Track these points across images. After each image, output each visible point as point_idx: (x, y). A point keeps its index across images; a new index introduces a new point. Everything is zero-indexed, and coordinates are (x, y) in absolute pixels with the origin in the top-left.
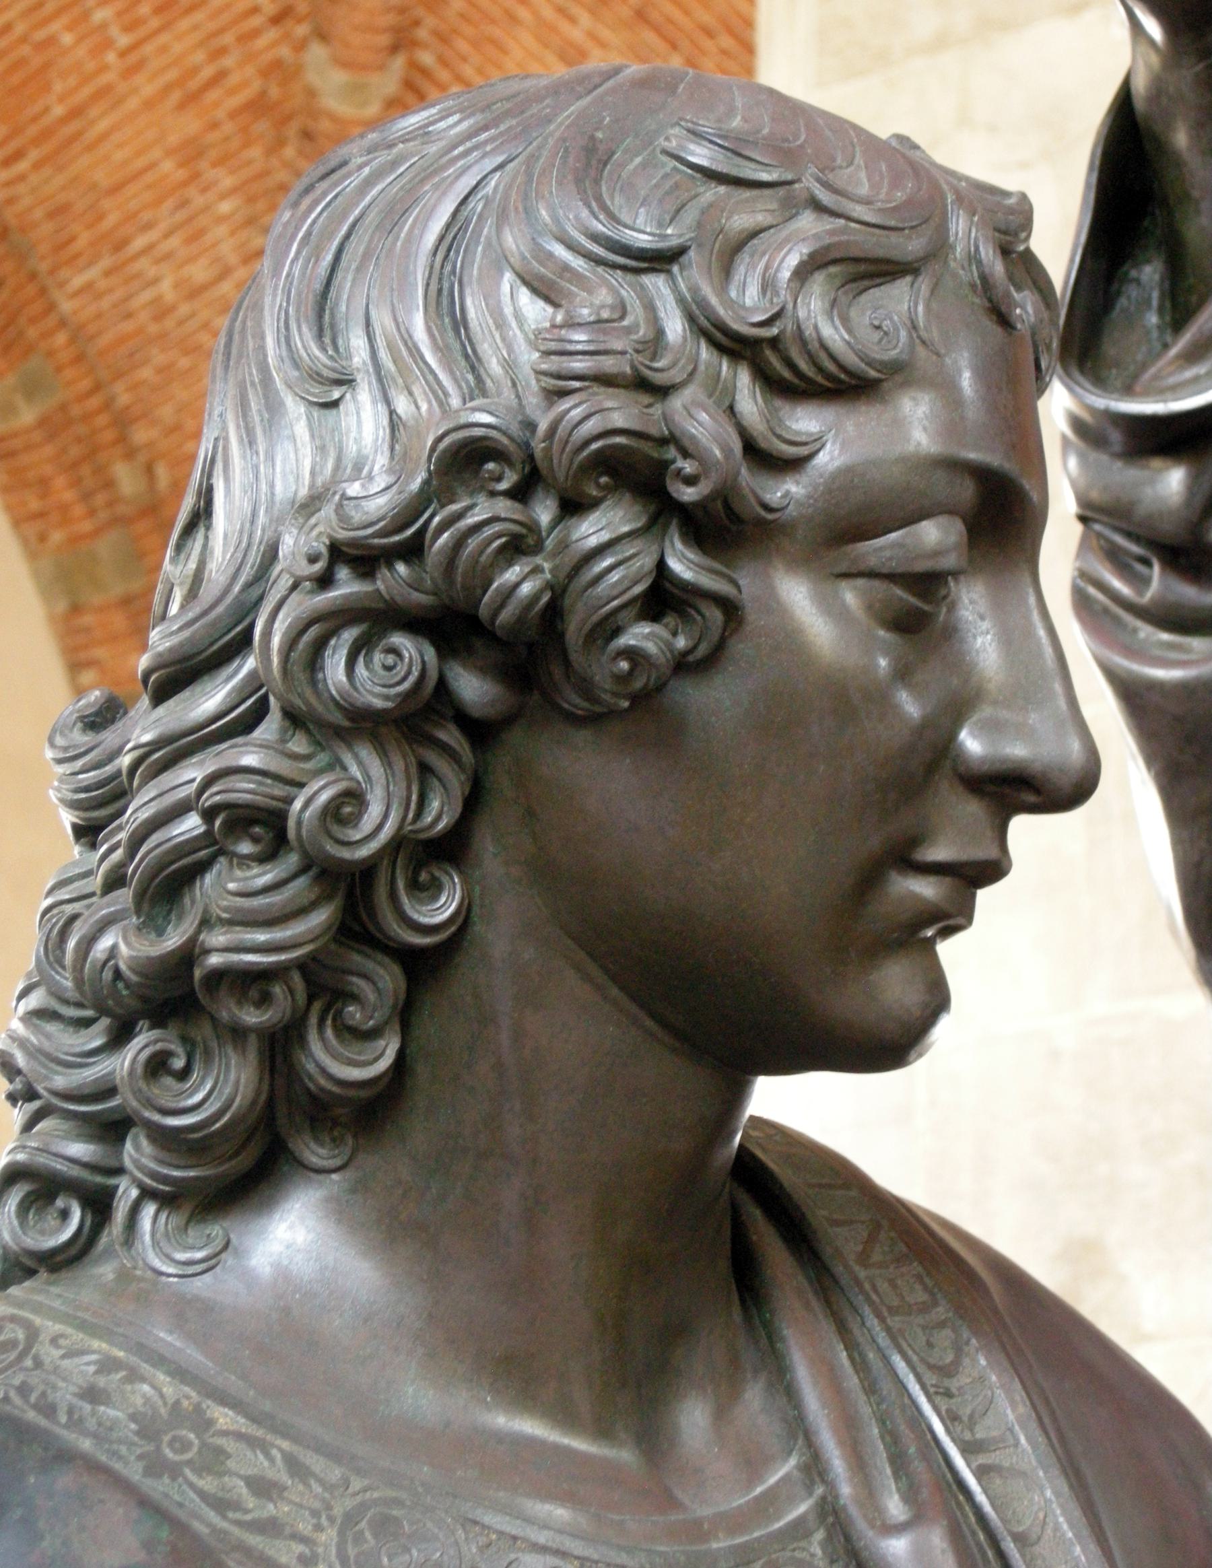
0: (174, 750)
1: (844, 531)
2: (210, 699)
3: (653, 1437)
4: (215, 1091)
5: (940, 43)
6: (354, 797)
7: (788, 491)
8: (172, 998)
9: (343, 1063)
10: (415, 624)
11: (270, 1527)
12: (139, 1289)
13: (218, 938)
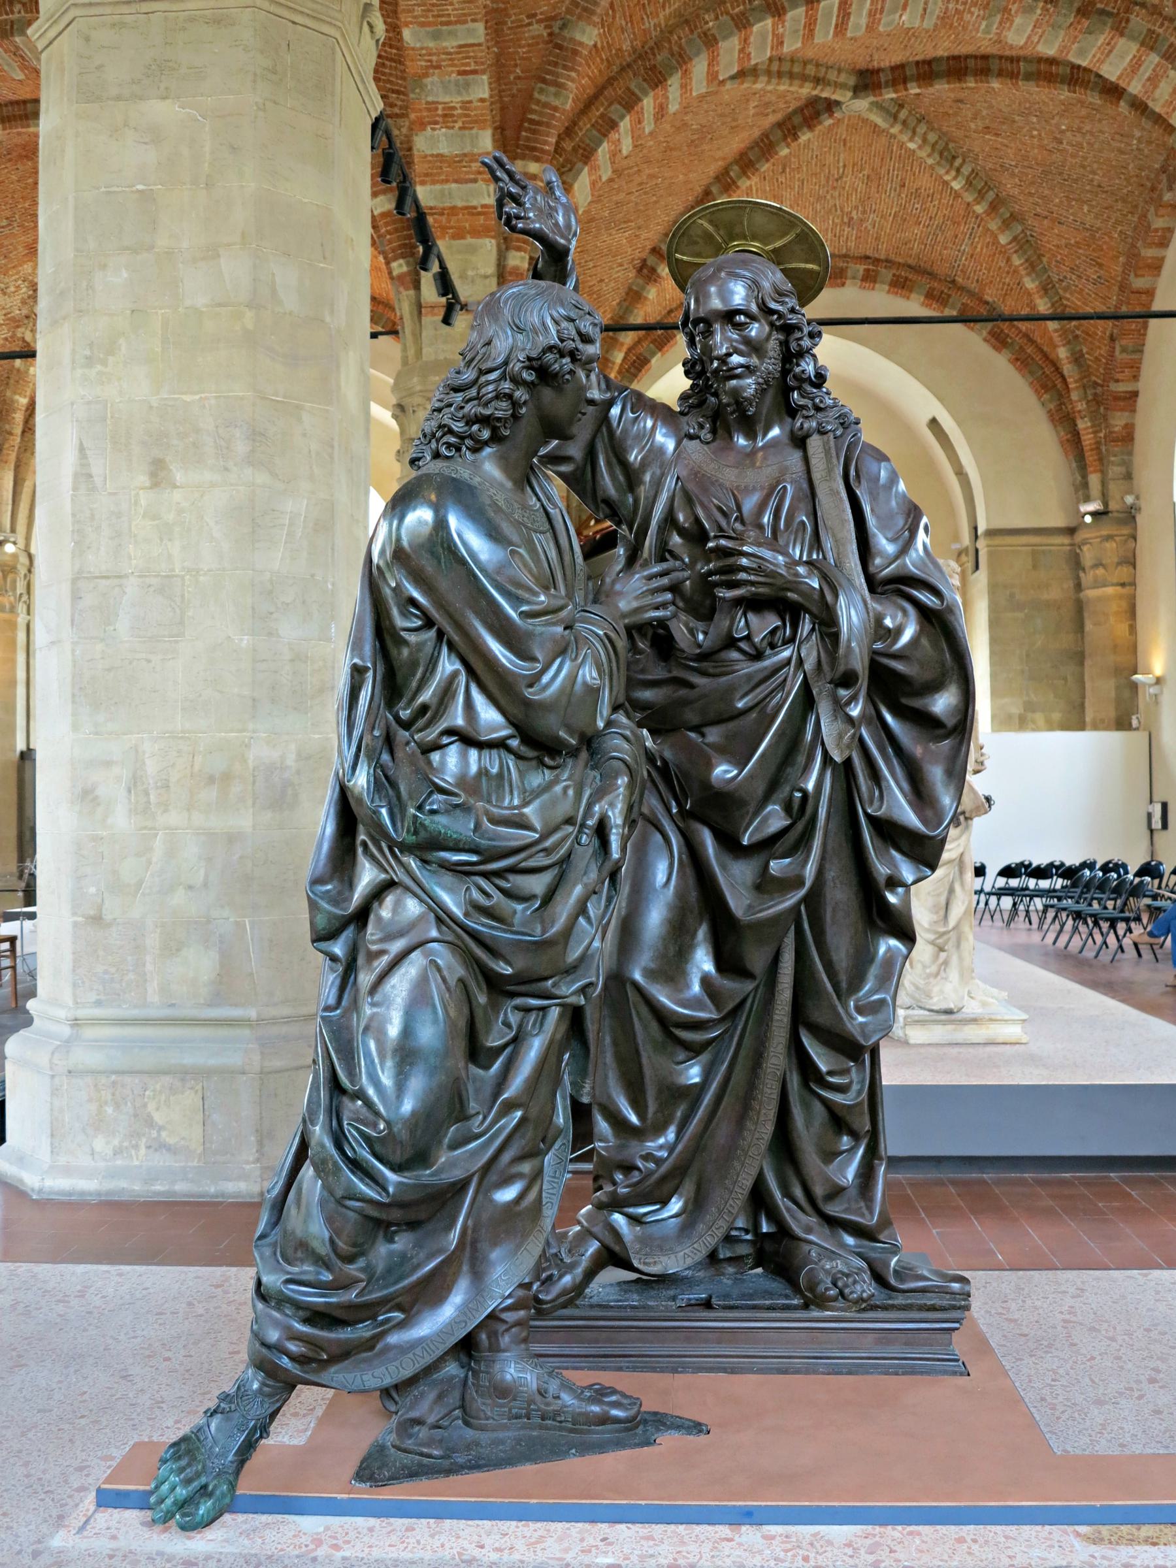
5: (118, 98)
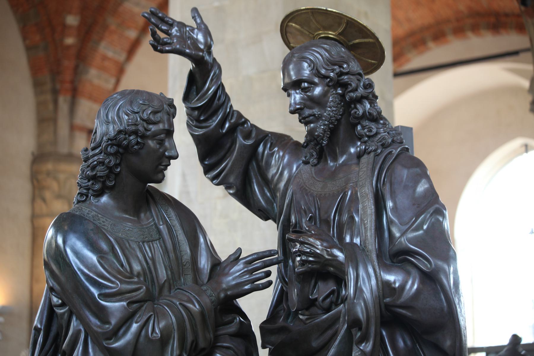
0: (94, 156)
1: (154, 136)
2: (97, 151)
3: (138, 217)
4: (97, 187)
6: (111, 161)
7: (148, 133)
8: (94, 178)
9: (110, 184)
10: (116, 145)
11: (104, 225)
12: (91, 204)
13: (98, 173)
